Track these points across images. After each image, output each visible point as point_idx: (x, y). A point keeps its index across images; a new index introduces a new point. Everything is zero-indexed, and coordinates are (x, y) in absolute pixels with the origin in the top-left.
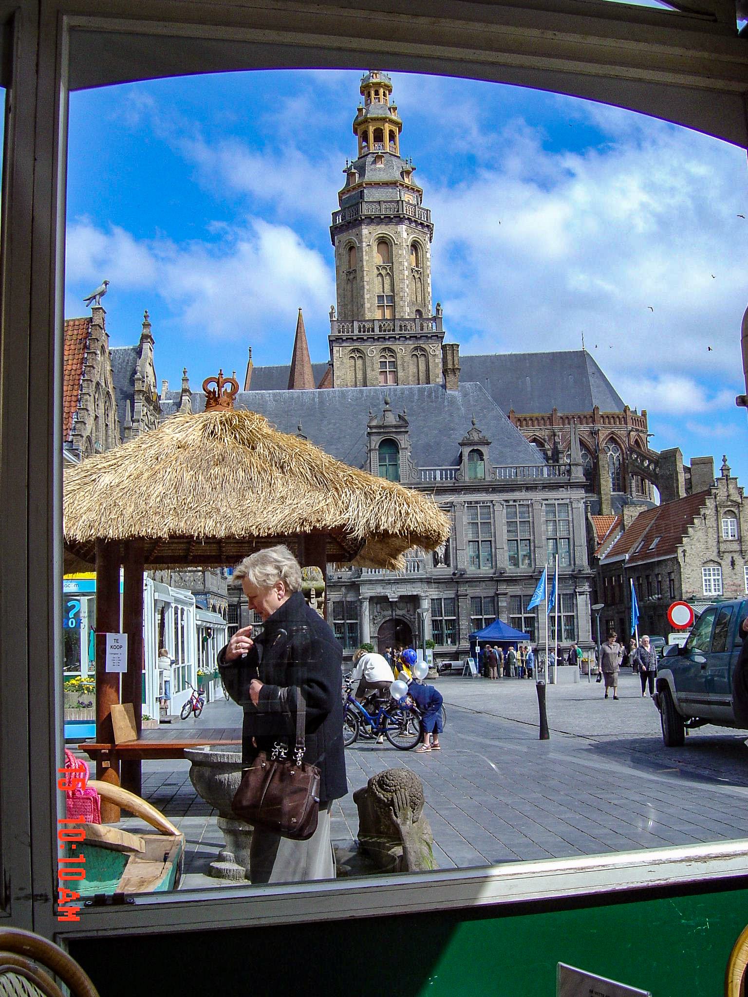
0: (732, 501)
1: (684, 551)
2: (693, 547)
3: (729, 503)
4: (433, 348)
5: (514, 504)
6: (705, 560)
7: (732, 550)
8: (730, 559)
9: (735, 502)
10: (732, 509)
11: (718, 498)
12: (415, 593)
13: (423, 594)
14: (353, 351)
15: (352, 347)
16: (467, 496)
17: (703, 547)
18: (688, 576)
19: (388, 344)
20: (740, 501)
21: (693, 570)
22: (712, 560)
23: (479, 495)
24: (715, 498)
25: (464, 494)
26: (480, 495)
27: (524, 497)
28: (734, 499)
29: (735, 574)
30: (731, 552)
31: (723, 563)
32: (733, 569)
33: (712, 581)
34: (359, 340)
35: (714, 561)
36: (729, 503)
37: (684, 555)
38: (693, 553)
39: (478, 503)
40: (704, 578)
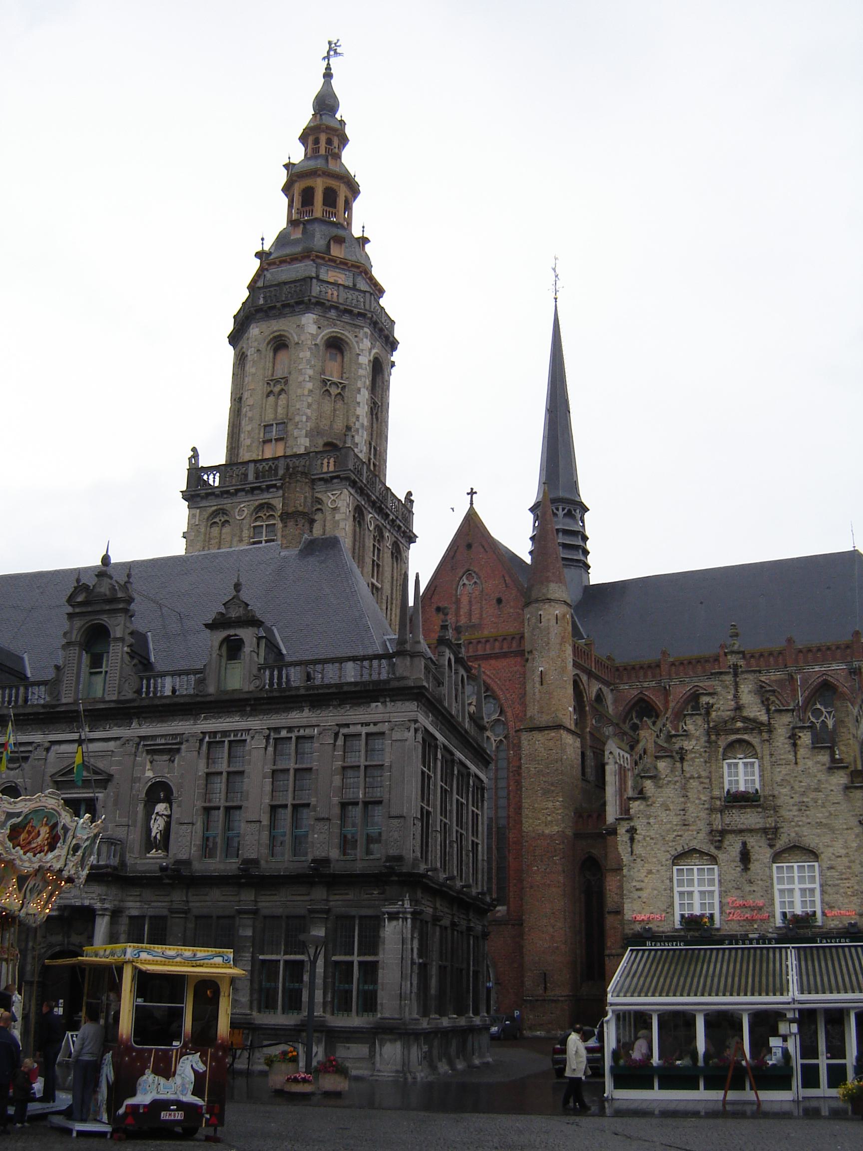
0: (746, 719)
1: (632, 831)
2: (652, 821)
3: (739, 724)
4: (333, 498)
5: (289, 735)
6: (680, 849)
7: (740, 826)
8: (738, 847)
9: (754, 720)
10: (746, 737)
11: (714, 714)
12: (87, 903)
13: (98, 905)
14: (215, 513)
15: (214, 508)
16: (208, 721)
17: (675, 820)
18: (638, 885)
19: (265, 497)
20: (764, 718)
21: (650, 872)
22: (694, 850)
23: (228, 720)
24: (708, 714)
25: (205, 719)
26: (231, 720)
27: (304, 722)
28: (752, 715)
29: (750, 882)
30: (741, 831)
31: (721, 856)
32: (746, 869)
33: (696, 896)
34: (225, 496)
35: (702, 853)
36: (739, 724)
37: (632, 840)
38: (652, 833)
39: (226, 737)
40: (677, 889)
